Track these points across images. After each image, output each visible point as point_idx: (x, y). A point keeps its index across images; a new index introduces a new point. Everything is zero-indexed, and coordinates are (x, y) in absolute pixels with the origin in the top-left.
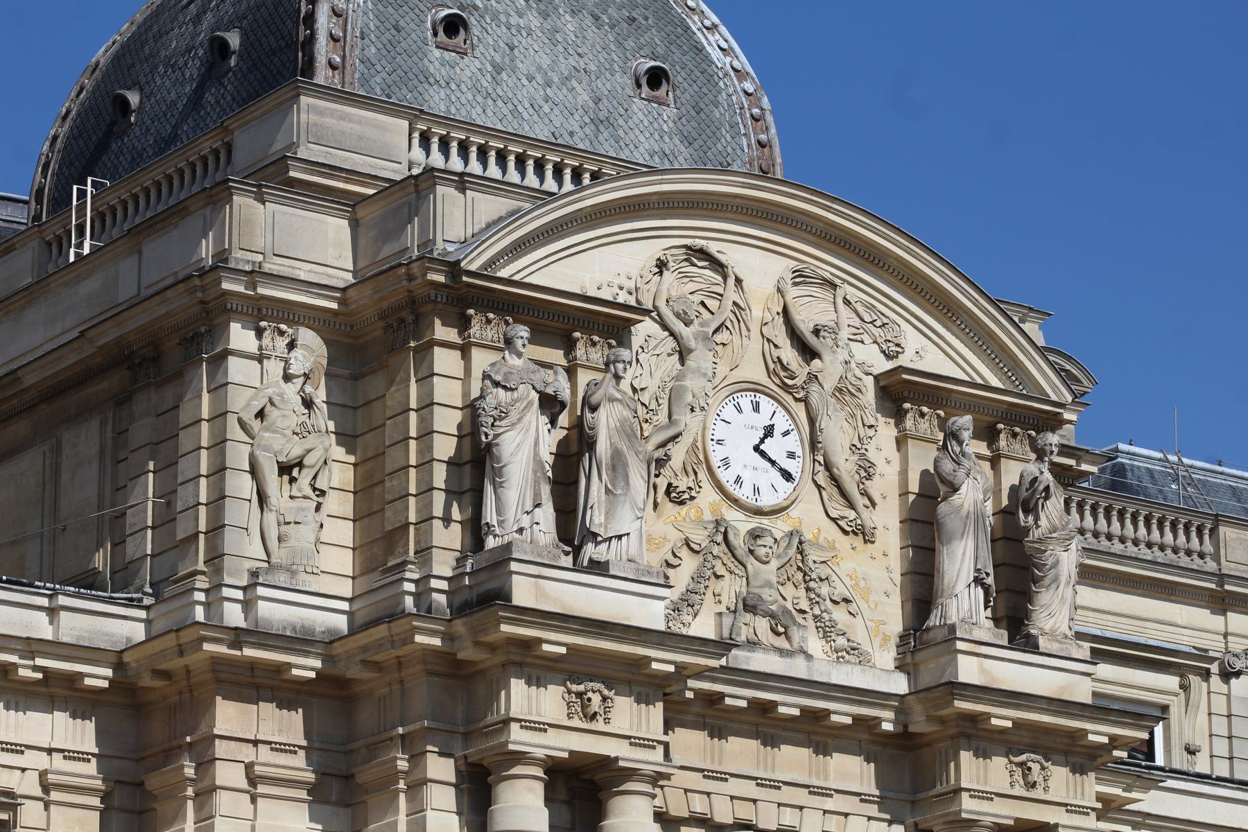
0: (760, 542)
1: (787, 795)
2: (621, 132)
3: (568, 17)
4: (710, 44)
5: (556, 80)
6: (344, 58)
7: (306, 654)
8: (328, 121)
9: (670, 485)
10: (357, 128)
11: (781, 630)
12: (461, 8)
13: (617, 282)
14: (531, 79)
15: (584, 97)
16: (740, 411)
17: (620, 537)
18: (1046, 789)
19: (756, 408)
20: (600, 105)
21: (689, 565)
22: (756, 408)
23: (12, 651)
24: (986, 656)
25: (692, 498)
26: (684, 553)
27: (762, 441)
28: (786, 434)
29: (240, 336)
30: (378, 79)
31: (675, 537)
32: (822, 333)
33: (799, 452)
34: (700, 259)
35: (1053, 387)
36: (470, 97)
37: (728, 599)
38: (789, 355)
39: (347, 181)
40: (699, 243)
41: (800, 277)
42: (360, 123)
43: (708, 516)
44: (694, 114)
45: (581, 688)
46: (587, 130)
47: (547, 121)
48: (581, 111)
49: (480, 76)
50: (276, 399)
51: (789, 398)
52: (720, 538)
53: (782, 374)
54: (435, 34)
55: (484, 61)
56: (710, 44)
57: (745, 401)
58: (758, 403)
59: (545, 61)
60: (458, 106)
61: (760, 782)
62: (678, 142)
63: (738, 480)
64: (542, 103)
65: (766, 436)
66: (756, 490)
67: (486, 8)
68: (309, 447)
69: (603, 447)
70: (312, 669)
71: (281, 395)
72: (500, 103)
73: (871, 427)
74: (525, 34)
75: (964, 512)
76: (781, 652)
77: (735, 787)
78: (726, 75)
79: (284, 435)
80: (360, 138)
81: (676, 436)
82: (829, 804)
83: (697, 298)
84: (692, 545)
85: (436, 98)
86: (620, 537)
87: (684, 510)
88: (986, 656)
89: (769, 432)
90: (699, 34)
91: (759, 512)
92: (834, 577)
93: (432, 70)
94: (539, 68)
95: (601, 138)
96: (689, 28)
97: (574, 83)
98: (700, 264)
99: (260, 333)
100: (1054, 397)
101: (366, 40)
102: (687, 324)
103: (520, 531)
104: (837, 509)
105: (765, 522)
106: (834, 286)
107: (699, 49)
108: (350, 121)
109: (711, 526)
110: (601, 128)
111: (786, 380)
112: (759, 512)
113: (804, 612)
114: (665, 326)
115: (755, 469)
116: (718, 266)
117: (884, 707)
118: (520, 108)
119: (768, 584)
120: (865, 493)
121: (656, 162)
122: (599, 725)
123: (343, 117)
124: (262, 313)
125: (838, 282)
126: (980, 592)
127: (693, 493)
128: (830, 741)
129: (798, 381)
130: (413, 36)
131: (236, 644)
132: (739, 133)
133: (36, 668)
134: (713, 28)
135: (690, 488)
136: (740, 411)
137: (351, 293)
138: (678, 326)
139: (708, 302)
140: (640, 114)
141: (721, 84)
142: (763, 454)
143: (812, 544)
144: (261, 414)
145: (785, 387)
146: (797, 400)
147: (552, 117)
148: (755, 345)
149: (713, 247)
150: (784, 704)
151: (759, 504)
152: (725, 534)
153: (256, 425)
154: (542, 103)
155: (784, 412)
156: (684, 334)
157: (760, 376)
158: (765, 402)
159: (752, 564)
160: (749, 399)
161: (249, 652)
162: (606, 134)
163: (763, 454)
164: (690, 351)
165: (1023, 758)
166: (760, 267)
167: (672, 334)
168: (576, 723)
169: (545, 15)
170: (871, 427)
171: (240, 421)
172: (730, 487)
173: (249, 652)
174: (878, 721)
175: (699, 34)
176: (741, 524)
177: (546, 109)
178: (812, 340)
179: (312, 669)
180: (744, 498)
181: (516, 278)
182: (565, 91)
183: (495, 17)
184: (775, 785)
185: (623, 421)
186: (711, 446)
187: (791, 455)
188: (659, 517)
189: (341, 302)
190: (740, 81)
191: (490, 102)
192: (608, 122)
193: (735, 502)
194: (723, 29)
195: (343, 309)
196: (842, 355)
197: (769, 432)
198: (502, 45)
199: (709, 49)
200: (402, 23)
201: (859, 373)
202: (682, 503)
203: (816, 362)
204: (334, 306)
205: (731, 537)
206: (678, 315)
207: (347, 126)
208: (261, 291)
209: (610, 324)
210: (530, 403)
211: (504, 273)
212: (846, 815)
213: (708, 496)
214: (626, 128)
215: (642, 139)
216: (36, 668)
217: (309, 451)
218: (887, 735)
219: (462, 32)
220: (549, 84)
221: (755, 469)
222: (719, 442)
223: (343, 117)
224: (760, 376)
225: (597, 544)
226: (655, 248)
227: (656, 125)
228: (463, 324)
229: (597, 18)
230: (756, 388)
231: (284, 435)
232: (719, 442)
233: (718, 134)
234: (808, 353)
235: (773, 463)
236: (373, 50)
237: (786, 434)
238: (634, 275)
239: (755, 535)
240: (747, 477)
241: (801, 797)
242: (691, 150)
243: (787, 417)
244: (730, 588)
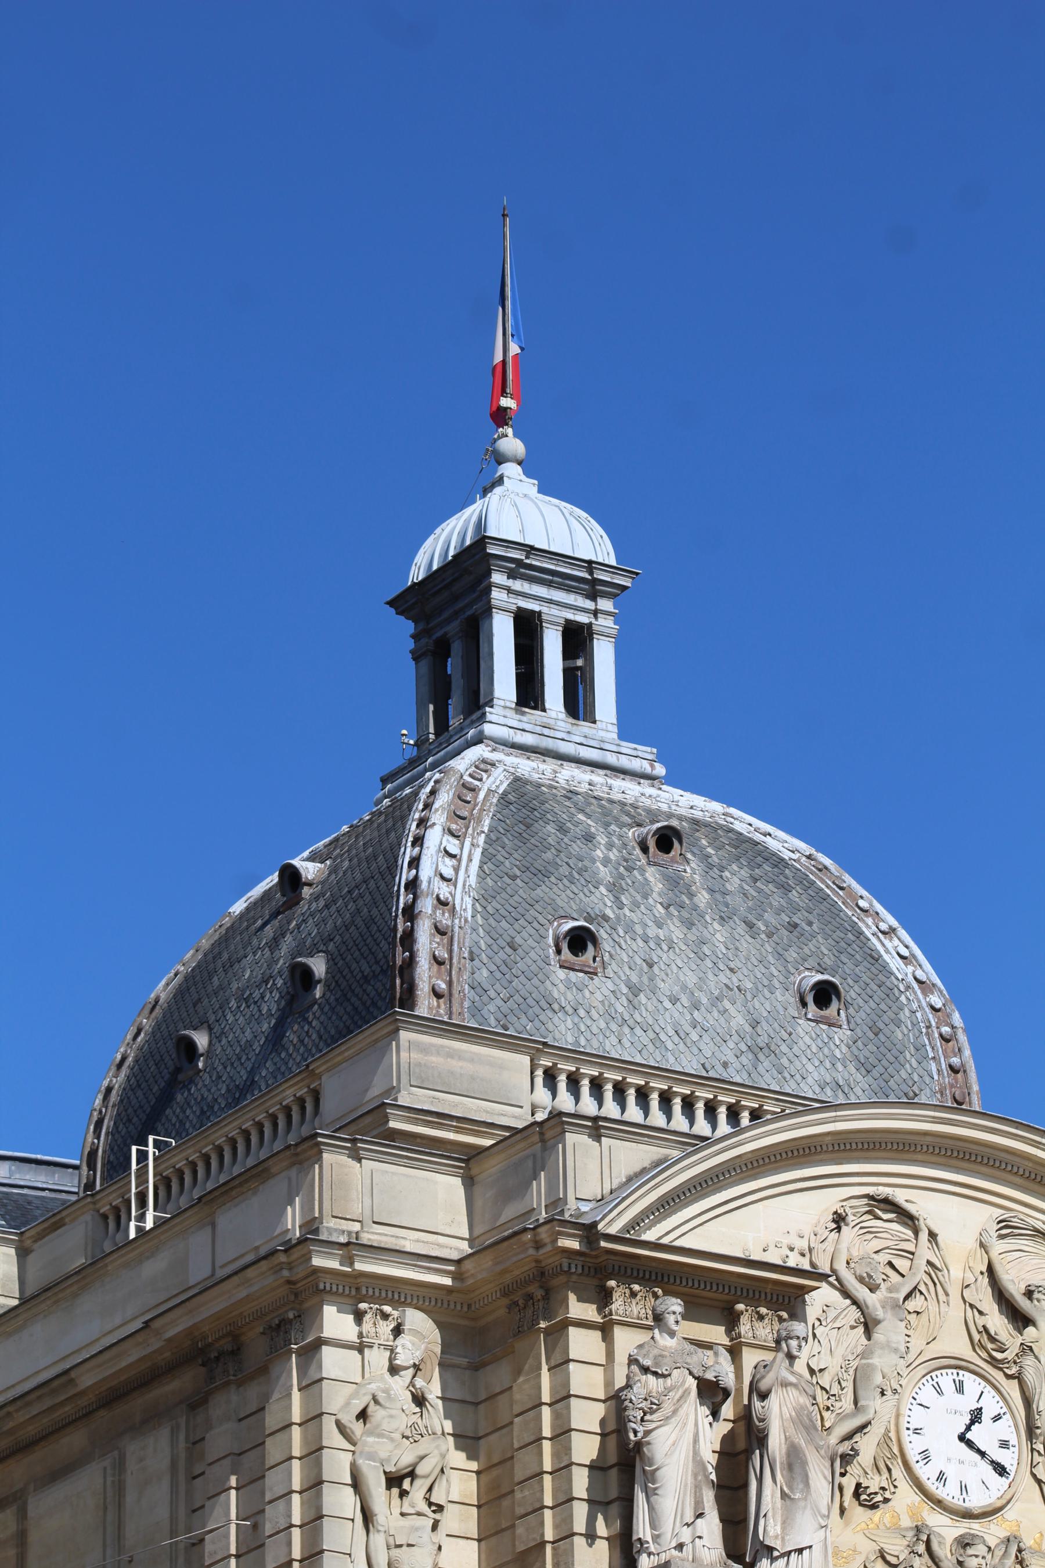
0: (970, 1551)
2: (784, 1061)
3: (716, 926)
4: (887, 951)
5: (704, 1000)
6: (450, 984)
8: (434, 1059)
9: (858, 1485)
10: (468, 1067)
12: (589, 919)
13: (785, 1241)
14: (674, 1000)
15: (739, 1020)
16: (940, 1393)
17: (800, 1551)
19: (960, 1388)
20: (759, 1029)
22: (960, 1388)
25: (886, 1500)
27: (968, 1428)
28: (997, 1418)
29: (336, 1322)
30: (492, 1007)
32: (1036, 1295)
33: (1013, 1440)
34: (885, 1211)
36: (603, 1025)
38: (997, 1322)
39: (458, 1130)
41: (1007, 1228)
42: (472, 1061)
43: (906, 1522)
44: (871, 1035)
46: (744, 1059)
47: (695, 1051)
48: (736, 1037)
49: (613, 1000)
50: (381, 1397)
51: (999, 1376)
52: (921, 1548)
53: (990, 1346)
54: (559, 952)
55: (618, 981)
56: (887, 951)
57: (946, 1379)
58: (961, 1383)
59: (691, 979)
60: (589, 1035)
62: (853, 1070)
63: (941, 1477)
64: (688, 1028)
65: (973, 1422)
66: (964, 1488)
67: (618, 918)
68: (422, 1453)
69: (776, 1442)
71: (386, 1391)
72: (638, 1031)
74: (665, 948)
78: (908, 987)
79: (392, 1440)
80: (473, 1078)
81: (864, 1427)
83: (883, 1258)
84: (889, 1558)
85: (562, 1028)
86: (800, 1551)
87: (877, 1514)
89: (976, 1417)
90: (874, 940)
91: (967, 1515)
93: (556, 994)
94: (684, 988)
95: (760, 1068)
96: (861, 933)
97: (727, 1004)
98: (885, 1216)
99: (359, 1317)
101: (476, 962)
102: (873, 1289)
103: (680, 1547)
105: (975, 1527)
107: (875, 958)
108: (460, 1058)
109: (911, 1533)
110: (761, 1056)
111: (994, 1354)
112: (967, 1515)
114: (846, 1294)
115: (961, 1462)
116: (907, 1218)
118: (663, 1036)
121: (828, 1095)
123: (451, 1054)
124: (360, 1293)
127: (887, 1495)
129: (1009, 1355)
130: (532, 954)
132: (926, 1057)
134: (890, 932)
135: (883, 1489)
136: (940, 1393)
137: (468, 1265)
138: (861, 1292)
139: (898, 1262)
140: (807, 1039)
141: (903, 998)
142: (970, 1444)
143: (1034, 1552)
144: (363, 1415)
145: (993, 1362)
146: (1009, 1377)
147: (702, 1046)
148: (956, 1311)
149: (900, 1196)
151: (967, 1505)
152: (928, 1543)
153: (357, 1428)
154: (688, 1028)
155: (993, 1392)
156: (869, 1302)
157: (965, 1351)
158: (968, 1378)
160: (950, 1378)
162: (766, 1064)
163: (970, 1444)
164: (877, 1322)
166: (958, 1217)
167: (855, 1302)
169: (689, 924)
171: (338, 1424)
172: (932, 1486)
175: (874, 940)
176: (946, 1530)
177: (694, 1036)
178: (1023, 1303)
180: (949, 1498)
181: (665, 1241)
182: (716, 1014)
183: (629, 929)
185: (800, 1410)
186: (907, 1437)
187: (1004, 1444)
188: (847, 1524)
189: (456, 1276)
190: (925, 995)
191: (626, 1030)
192: (768, 1049)
193: (939, 1503)
194: (902, 933)
195: (458, 1285)
197: (976, 1417)
198: (639, 961)
199: (886, 957)
200: (518, 940)
202: (874, 1507)
203: (1030, 1330)
204: (447, 1281)
205: (935, 1546)
206: (861, 1280)
207: (455, 1065)
208: (360, 1266)
209: (780, 1293)
210: (686, 1392)
211: (650, 1236)
213: (905, 1497)
214: (791, 1055)
215: (811, 1068)
217: (422, 1458)
219: (590, 947)
220: (696, 1006)
221: (961, 1462)
222: (917, 1431)
223: (451, 1054)
224: (965, 1351)
225: (774, 1560)
226: (830, 1200)
227: (826, 1050)
228: (603, 1299)
229: (750, 926)
230: (959, 1365)
231: (392, 1440)
232: (917, 1431)
233: (901, 1059)
234: (1020, 1319)
235: (982, 1454)
236: (485, 973)
237: (997, 1418)
238: (807, 1231)
239: (964, 1543)
240: (949, 1474)
242: (869, 1078)
243: (997, 1398)
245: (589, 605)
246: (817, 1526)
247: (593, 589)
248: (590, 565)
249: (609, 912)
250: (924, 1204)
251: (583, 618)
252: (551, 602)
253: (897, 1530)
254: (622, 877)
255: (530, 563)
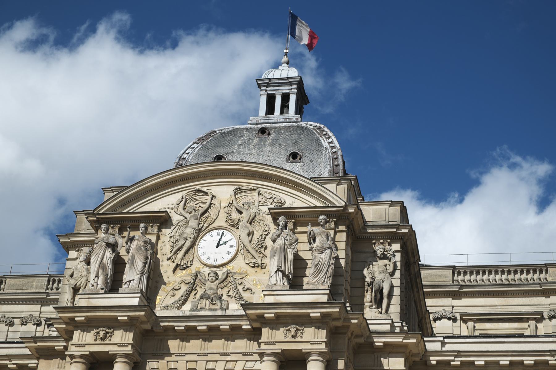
1: (210, 357)
4: (325, 142)
7: (59, 341)
11: (214, 302)
17: (130, 281)
18: (302, 337)
21: (184, 288)
23: (5, 360)
24: (278, 295)
25: (187, 267)
26: (183, 285)
31: (179, 280)
35: (338, 201)
37: (198, 296)
38: (235, 215)
40: (198, 187)
43: (194, 271)
45: (98, 330)
56: (325, 142)
61: (199, 355)
63: (208, 258)
70: (62, 346)
73: (266, 231)
75: (275, 249)
76: (211, 310)
77: (188, 358)
82: (228, 358)
86: (130, 281)
87: (184, 272)
88: (278, 295)
92: (245, 282)
96: (319, 140)
98: (200, 194)
100: (338, 205)
104: (250, 259)
106: (255, 190)
112: (215, 267)
113: (230, 296)
116: (206, 194)
117: (242, 320)
119: (211, 289)
120: (260, 252)
122: (107, 342)
125: (255, 188)
126: (280, 274)
128: (230, 337)
129: (235, 223)
131: (36, 343)
133: (14, 364)
136: (212, 236)
138: (188, 215)
143: (236, 273)
144: (72, 276)
145: (231, 225)
150: (199, 326)
159: (208, 284)
161: (39, 344)
165: (289, 327)
168: (98, 342)
170: (266, 231)
173: (39, 344)
174: (240, 327)
176: (206, 271)
179: (62, 346)
184: (206, 355)
187: (232, 246)
193: (205, 265)
194: (333, 137)
196: (253, 211)
201: (264, 215)
208: (71, 239)
212: (237, 361)
216: (14, 364)
218: (247, 331)
222: (202, 248)
229: (280, 145)
232: (202, 248)
234: (241, 213)
239: (209, 274)
240: (212, 257)
241: (217, 357)
244: (200, 292)
245: (290, 87)
246: (135, 274)
247: (290, 84)
248: (287, 78)
249: (235, 151)
250: (214, 190)
251: (288, 91)
252: (279, 90)
253: (190, 275)
254: (245, 142)
255: (270, 83)
